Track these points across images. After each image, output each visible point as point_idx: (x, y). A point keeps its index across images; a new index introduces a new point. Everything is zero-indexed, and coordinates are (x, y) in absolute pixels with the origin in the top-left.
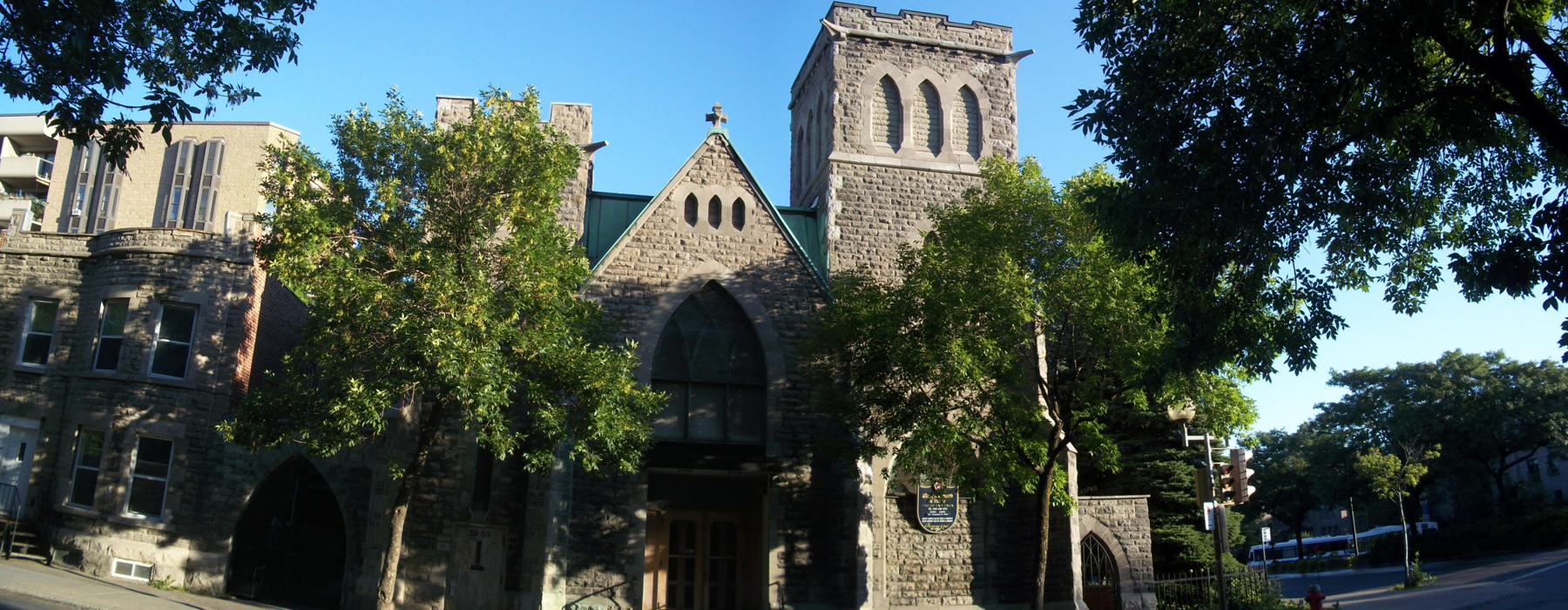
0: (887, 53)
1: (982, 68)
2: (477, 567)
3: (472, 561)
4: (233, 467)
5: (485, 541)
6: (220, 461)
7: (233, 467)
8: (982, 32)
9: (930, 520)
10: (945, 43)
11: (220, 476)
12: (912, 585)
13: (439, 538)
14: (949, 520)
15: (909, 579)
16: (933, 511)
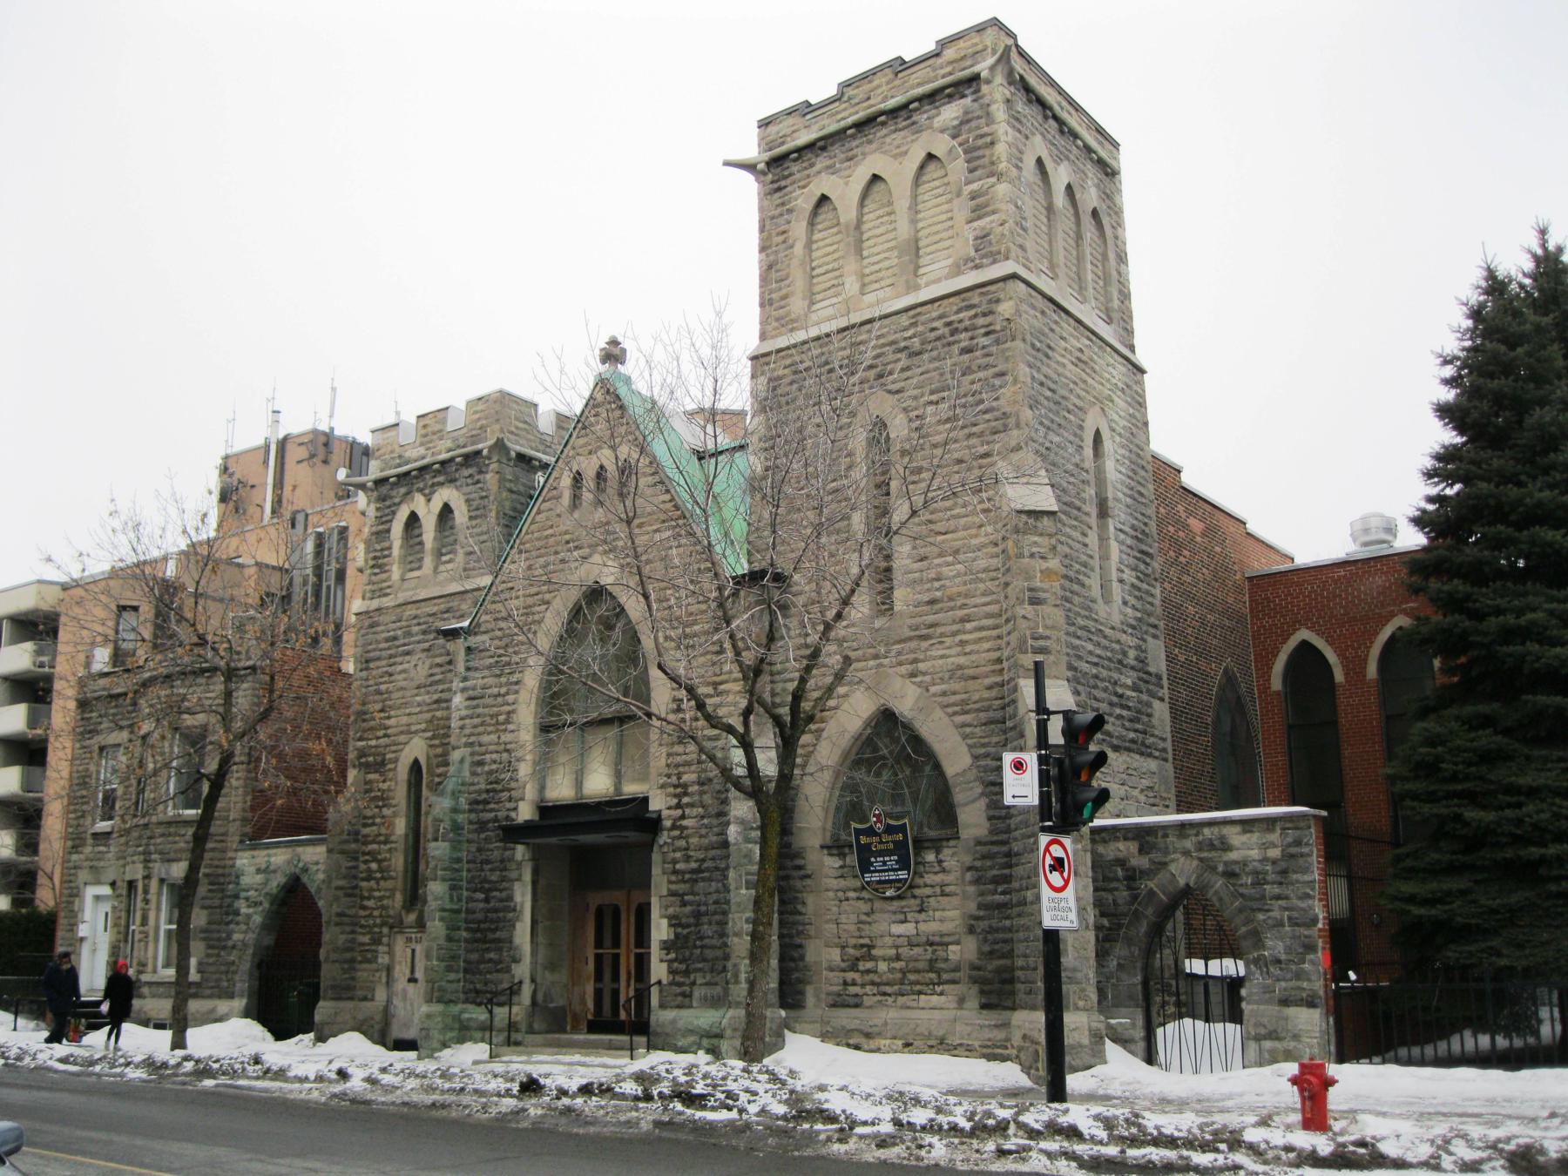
0: (821, 162)
1: (950, 113)
2: (412, 980)
3: (408, 975)
4: (247, 899)
5: (419, 948)
6: (237, 897)
7: (247, 899)
8: (950, 53)
9: (876, 877)
10: (891, 103)
11: (237, 913)
12: (856, 976)
13: (381, 948)
14: (903, 875)
15: (853, 968)
16: (877, 862)
